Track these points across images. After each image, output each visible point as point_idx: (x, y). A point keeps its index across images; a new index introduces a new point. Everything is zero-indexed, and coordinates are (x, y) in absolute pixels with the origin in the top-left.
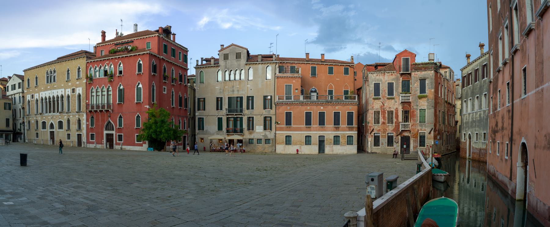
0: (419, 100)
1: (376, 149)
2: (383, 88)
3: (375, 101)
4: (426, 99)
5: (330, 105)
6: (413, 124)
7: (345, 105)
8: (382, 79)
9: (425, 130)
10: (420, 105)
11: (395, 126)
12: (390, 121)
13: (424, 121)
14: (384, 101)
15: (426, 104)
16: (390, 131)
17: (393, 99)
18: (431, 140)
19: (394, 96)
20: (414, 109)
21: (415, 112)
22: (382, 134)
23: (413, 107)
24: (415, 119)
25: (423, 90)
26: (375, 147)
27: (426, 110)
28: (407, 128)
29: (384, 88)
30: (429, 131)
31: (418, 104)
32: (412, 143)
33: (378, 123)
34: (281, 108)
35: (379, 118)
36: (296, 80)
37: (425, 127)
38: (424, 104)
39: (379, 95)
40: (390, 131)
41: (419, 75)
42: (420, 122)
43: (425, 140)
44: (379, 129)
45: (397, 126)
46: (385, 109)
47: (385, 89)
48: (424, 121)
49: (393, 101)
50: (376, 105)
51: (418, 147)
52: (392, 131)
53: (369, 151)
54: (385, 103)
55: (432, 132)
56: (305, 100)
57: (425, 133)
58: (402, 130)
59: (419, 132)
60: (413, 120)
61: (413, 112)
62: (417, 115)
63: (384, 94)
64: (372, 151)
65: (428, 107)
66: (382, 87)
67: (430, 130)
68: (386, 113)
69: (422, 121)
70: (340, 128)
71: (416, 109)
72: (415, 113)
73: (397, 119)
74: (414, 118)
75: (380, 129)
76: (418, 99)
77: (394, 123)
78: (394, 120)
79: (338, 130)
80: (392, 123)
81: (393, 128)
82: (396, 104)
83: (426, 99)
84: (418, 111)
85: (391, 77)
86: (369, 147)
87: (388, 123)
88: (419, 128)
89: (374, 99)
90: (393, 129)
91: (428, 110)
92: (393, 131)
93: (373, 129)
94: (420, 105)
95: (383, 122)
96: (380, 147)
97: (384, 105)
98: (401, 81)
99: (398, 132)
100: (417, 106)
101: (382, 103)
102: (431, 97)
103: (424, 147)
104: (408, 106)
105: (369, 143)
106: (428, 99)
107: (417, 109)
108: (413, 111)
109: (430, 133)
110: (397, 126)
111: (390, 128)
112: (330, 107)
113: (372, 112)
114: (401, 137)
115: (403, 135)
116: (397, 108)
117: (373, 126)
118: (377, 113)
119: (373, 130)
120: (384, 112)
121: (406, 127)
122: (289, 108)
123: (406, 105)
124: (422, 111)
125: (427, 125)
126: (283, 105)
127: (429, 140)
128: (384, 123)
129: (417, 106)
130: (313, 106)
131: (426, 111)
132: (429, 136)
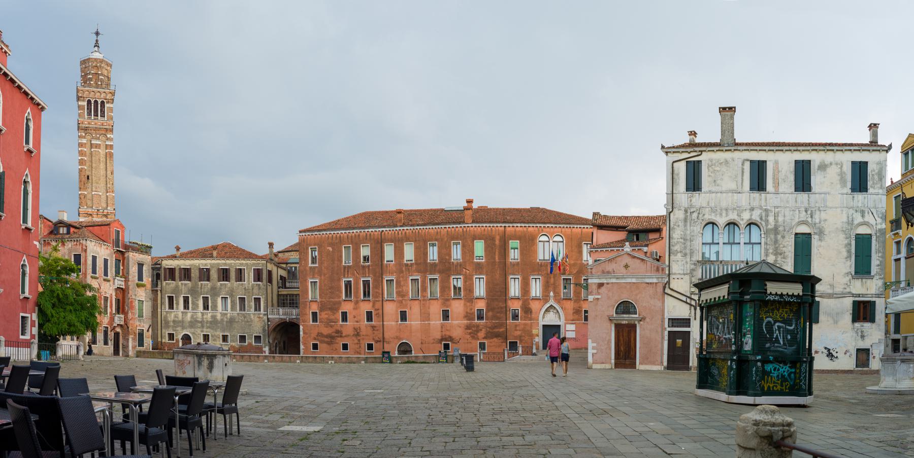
0: (137, 289)
4: (143, 289)
6: (132, 318)
9: (143, 327)
15: (144, 295)
24: (133, 311)
25: (140, 278)
30: (147, 329)
37: (144, 323)
42: (138, 316)
43: (143, 338)
45: (112, 319)
48: (141, 315)
52: (107, 325)
55: (150, 330)
57: (143, 330)
59: (138, 328)
60: (131, 313)
61: (131, 302)
65: (145, 299)
67: (148, 327)
69: (141, 316)
73: (112, 310)
77: (109, 314)
81: (108, 320)
88: (138, 323)
90: (109, 322)
109: (148, 331)
110: (112, 319)
124: (141, 302)
125: (145, 321)
127: (147, 339)
129: (136, 295)
132: (148, 334)
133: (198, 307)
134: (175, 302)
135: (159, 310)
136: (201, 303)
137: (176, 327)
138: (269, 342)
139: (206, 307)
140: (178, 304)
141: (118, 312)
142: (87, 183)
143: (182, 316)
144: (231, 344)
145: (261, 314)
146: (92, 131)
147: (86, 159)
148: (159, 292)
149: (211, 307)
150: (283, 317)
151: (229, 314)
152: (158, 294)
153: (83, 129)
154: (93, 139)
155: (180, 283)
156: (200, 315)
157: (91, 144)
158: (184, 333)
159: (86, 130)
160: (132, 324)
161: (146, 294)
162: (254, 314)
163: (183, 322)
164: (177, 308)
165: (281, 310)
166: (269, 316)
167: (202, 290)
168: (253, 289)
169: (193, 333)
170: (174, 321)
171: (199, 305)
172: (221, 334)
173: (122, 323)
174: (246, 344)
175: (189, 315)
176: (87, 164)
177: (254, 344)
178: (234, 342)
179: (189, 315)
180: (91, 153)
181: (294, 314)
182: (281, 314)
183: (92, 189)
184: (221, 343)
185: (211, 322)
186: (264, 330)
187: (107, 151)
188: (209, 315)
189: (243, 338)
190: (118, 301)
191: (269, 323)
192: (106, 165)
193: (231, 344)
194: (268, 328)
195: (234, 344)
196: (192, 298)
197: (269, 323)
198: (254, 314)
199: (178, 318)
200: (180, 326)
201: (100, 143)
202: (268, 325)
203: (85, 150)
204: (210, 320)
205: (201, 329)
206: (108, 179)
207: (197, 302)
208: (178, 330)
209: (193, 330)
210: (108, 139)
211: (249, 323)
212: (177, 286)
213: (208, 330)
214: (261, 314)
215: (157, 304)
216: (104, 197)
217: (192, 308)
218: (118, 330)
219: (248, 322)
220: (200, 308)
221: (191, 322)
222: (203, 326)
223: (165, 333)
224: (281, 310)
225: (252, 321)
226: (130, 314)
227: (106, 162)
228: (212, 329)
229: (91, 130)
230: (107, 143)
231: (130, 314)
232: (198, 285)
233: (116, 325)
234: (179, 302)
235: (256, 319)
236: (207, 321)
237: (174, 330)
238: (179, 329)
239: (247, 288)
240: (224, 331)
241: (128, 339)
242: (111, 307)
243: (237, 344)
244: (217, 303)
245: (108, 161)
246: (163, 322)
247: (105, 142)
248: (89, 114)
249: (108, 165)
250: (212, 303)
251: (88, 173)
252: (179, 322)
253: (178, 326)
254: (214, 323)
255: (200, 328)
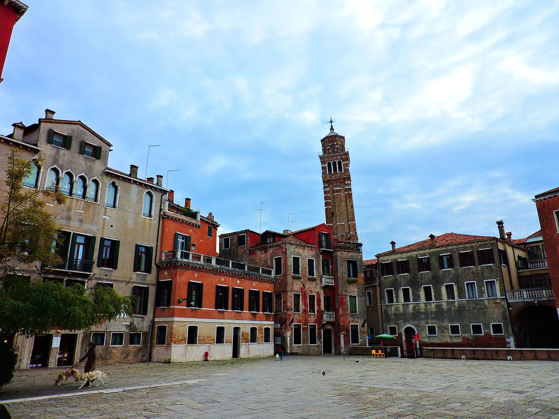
1: (296, 348)
2: (303, 264)
3: (295, 281)
5: (248, 279)
6: (343, 314)
7: (263, 282)
8: (302, 253)
9: (357, 322)
10: (350, 290)
11: (318, 315)
12: (312, 309)
13: (354, 311)
14: (305, 281)
15: (356, 290)
16: (311, 323)
17: (314, 280)
18: (365, 335)
19: (315, 276)
20: (343, 295)
21: (344, 299)
22: (303, 326)
23: (341, 292)
26: (295, 345)
27: (357, 297)
28: (331, 319)
29: (303, 264)
31: (347, 289)
32: (343, 338)
33: (298, 311)
34: (185, 274)
35: (299, 304)
36: (194, 229)
37: (357, 318)
38: (354, 290)
39: (299, 274)
40: (312, 322)
41: (346, 255)
44: (300, 319)
46: (306, 293)
47: (305, 266)
48: (354, 311)
49: (314, 283)
50: (297, 286)
51: (351, 344)
52: (314, 323)
53: (289, 352)
54: (305, 284)
55: (366, 325)
56: (218, 266)
58: (326, 322)
59: (350, 324)
61: (342, 299)
62: (347, 302)
63: (304, 273)
64: (293, 352)
65: (358, 294)
66: (302, 263)
68: (307, 298)
69: (354, 310)
70: (257, 316)
71: (345, 295)
72: (344, 300)
74: (343, 306)
75: (300, 320)
76: (347, 283)
78: (316, 308)
79: (255, 319)
80: (314, 312)
82: (317, 286)
83: (355, 285)
84: (347, 298)
85: (311, 252)
86: (288, 345)
87: (310, 312)
88: (350, 319)
89: (294, 278)
90: (315, 320)
91: (360, 298)
92: (315, 323)
93: (293, 319)
94: (350, 290)
95: (304, 310)
96: (302, 345)
97: (305, 287)
98: (321, 260)
99: (321, 324)
100: (346, 291)
101: (303, 284)
102: (361, 282)
103: (357, 344)
104: (329, 290)
105: (289, 339)
106: (358, 285)
107: (347, 296)
108: (342, 297)
109: (363, 326)
111: (312, 319)
112: (247, 282)
113: (291, 295)
114: (323, 331)
115: (326, 328)
116: (319, 292)
117: (292, 314)
118: (297, 297)
119: (292, 321)
120: (304, 296)
121: (330, 318)
122: (196, 275)
123: (327, 289)
124: (353, 298)
125: (359, 316)
126: (188, 269)
127: (362, 335)
128: (305, 311)
129: (346, 291)
130: (229, 278)
131: (357, 298)
133: (420, 297)
134: (394, 295)
135: (379, 305)
136: (422, 293)
137: (397, 320)
138: (513, 331)
139: (428, 297)
140: (397, 297)
141: (328, 307)
142: (332, 218)
143: (403, 309)
144: (463, 335)
145: (498, 299)
146: (334, 182)
147: (330, 201)
148: (378, 288)
149: (435, 296)
150: (529, 300)
151: (456, 303)
152: (376, 289)
153: (326, 182)
154: (334, 187)
155: (398, 276)
156: (422, 306)
157: (333, 190)
158: (409, 326)
159: (329, 182)
160: (343, 321)
161: (359, 289)
162: (488, 300)
163: (404, 314)
164: (397, 301)
165: (525, 292)
166: (509, 301)
167: (423, 280)
168: (483, 272)
169: (416, 326)
170: (395, 315)
171: (421, 296)
172: (450, 325)
173: (332, 320)
174: (483, 334)
175: (411, 307)
176: (332, 204)
177: (492, 334)
178: (466, 333)
179: (411, 307)
180: (334, 197)
181: (545, 295)
182: (526, 297)
183: (336, 221)
184: (451, 335)
185: (436, 312)
186: (504, 318)
187: (346, 193)
188: (433, 305)
189: (477, 329)
190: (327, 299)
191: (511, 309)
192: (347, 203)
193: (463, 335)
194: (509, 314)
195: (466, 335)
196: (412, 290)
197: (511, 309)
198: (488, 300)
199: (399, 310)
200: (402, 319)
201: (340, 188)
202: (509, 311)
203: (329, 195)
204: (435, 310)
205: (425, 321)
206: (349, 213)
207: (418, 293)
208: (400, 323)
209: (416, 322)
210: (346, 185)
211: (481, 309)
212: (395, 280)
213: (433, 321)
214: (498, 299)
215: (377, 299)
216: (346, 225)
217: (413, 299)
218: (329, 327)
219: (481, 309)
220: (421, 298)
221: (413, 314)
222: (427, 318)
223: (386, 327)
224: (525, 292)
225: (486, 307)
226: (341, 310)
227: (347, 201)
228: (438, 320)
229: (332, 181)
230: (346, 188)
231: (341, 310)
232: (418, 275)
233: (325, 322)
234: (398, 294)
235: (492, 305)
236: (431, 312)
237: (395, 324)
238: (401, 322)
239: (475, 272)
240: (452, 322)
241: (340, 336)
242: (319, 305)
243: (471, 334)
244: (440, 292)
245: (348, 200)
246: (384, 316)
247: (344, 187)
248: (330, 170)
249: (348, 202)
250: (435, 292)
251: (332, 211)
252: (401, 314)
253: (400, 319)
254: (439, 313)
255: (423, 319)
